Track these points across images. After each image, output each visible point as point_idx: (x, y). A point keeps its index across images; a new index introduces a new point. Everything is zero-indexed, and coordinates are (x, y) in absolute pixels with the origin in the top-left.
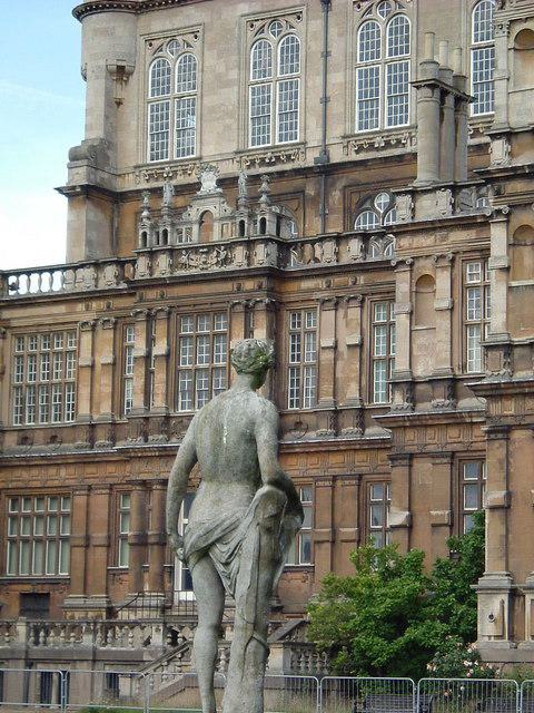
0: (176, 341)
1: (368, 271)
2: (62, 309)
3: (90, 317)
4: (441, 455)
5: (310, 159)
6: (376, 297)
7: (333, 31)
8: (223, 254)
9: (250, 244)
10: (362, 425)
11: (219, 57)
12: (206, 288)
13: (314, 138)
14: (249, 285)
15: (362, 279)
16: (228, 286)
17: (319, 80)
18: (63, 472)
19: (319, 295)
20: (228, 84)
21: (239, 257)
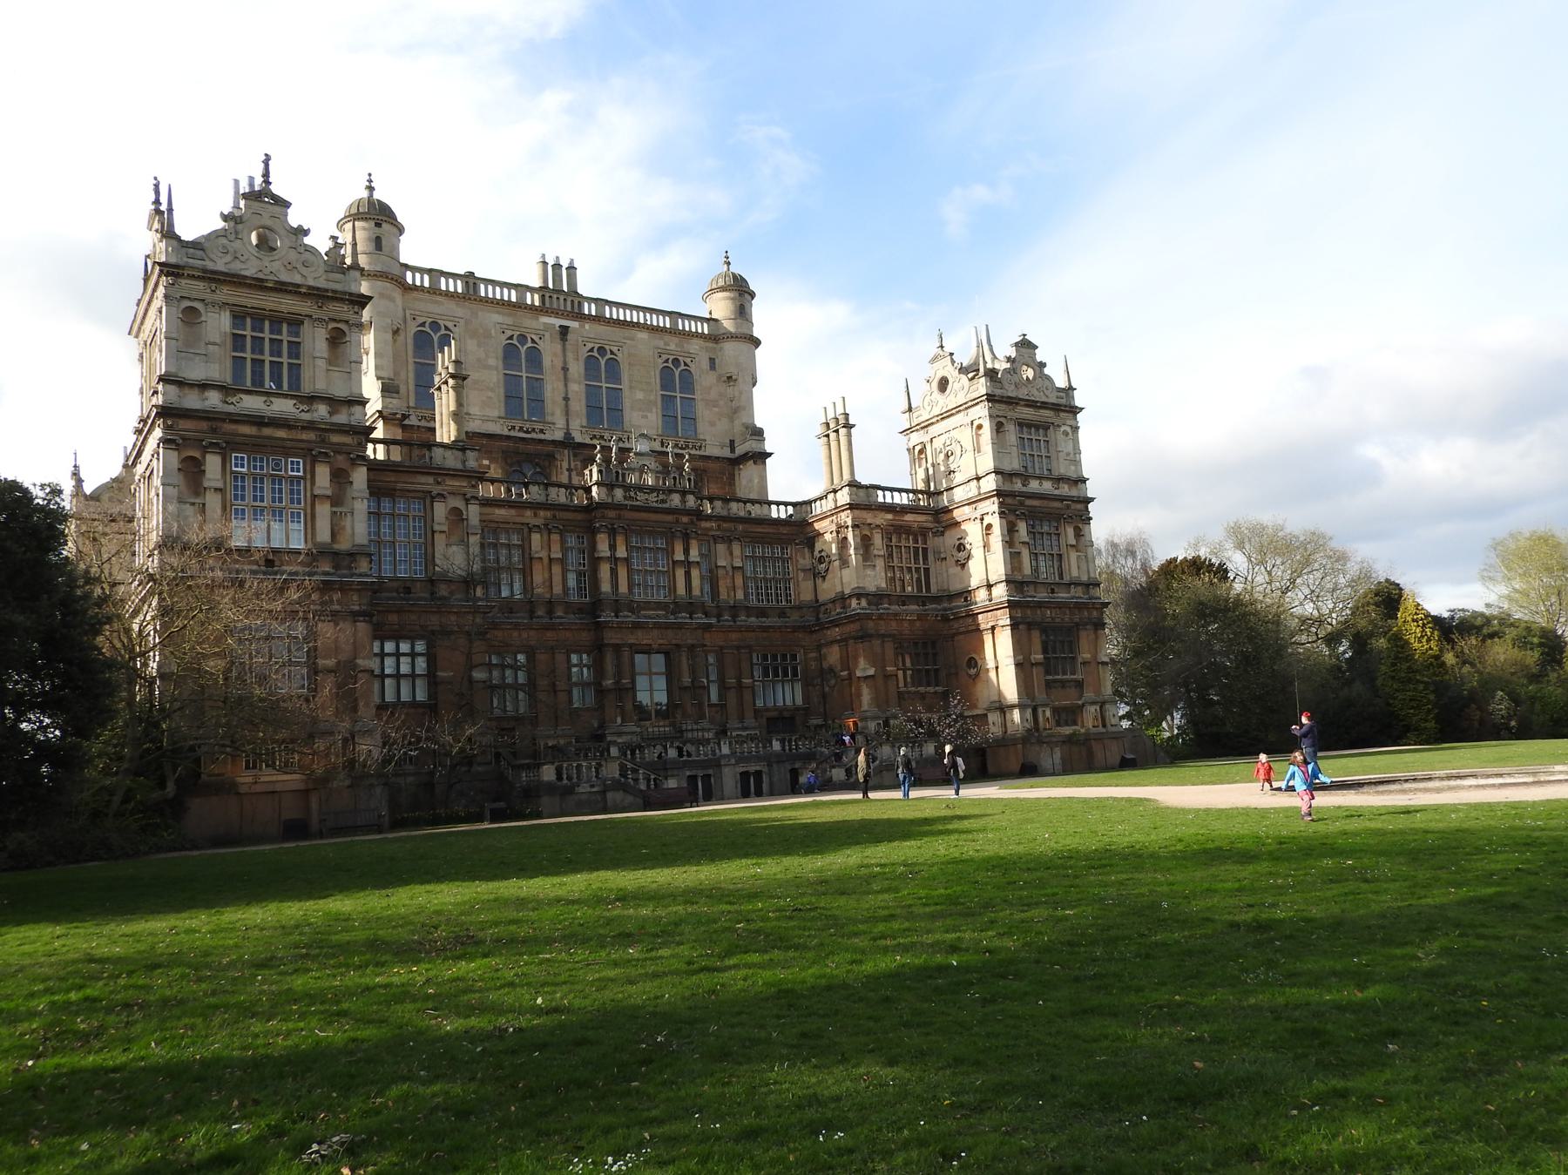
0: (629, 548)
1: (745, 523)
2: (513, 512)
3: (539, 522)
4: (890, 636)
5: (559, 435)
6: (747, 540)
7: (570, 355)
8: (661, 497)
9: (684, 493)
10: (748, 616)
11: (479, 345)
12: (644, 515)
13: (561, 423)
14: (685, 519)
15: (740, 527)
16: (670, 518)
17: (561, 385)
18: (525, 635)
19: (713, 533)
20: (489, 367)
21: (676, 500)
